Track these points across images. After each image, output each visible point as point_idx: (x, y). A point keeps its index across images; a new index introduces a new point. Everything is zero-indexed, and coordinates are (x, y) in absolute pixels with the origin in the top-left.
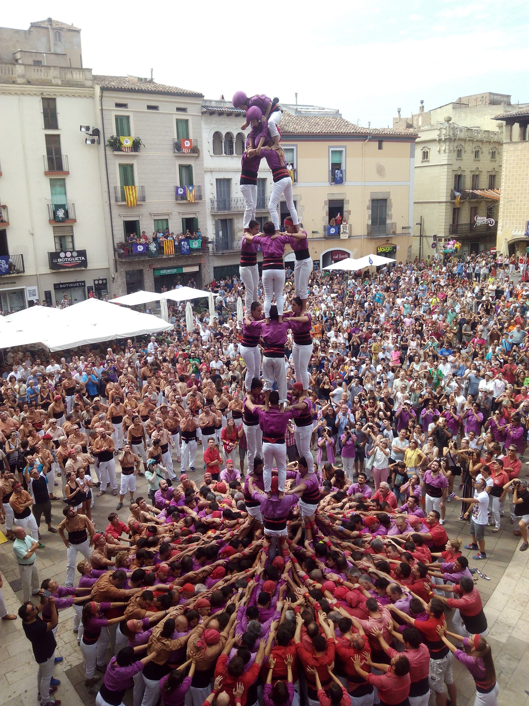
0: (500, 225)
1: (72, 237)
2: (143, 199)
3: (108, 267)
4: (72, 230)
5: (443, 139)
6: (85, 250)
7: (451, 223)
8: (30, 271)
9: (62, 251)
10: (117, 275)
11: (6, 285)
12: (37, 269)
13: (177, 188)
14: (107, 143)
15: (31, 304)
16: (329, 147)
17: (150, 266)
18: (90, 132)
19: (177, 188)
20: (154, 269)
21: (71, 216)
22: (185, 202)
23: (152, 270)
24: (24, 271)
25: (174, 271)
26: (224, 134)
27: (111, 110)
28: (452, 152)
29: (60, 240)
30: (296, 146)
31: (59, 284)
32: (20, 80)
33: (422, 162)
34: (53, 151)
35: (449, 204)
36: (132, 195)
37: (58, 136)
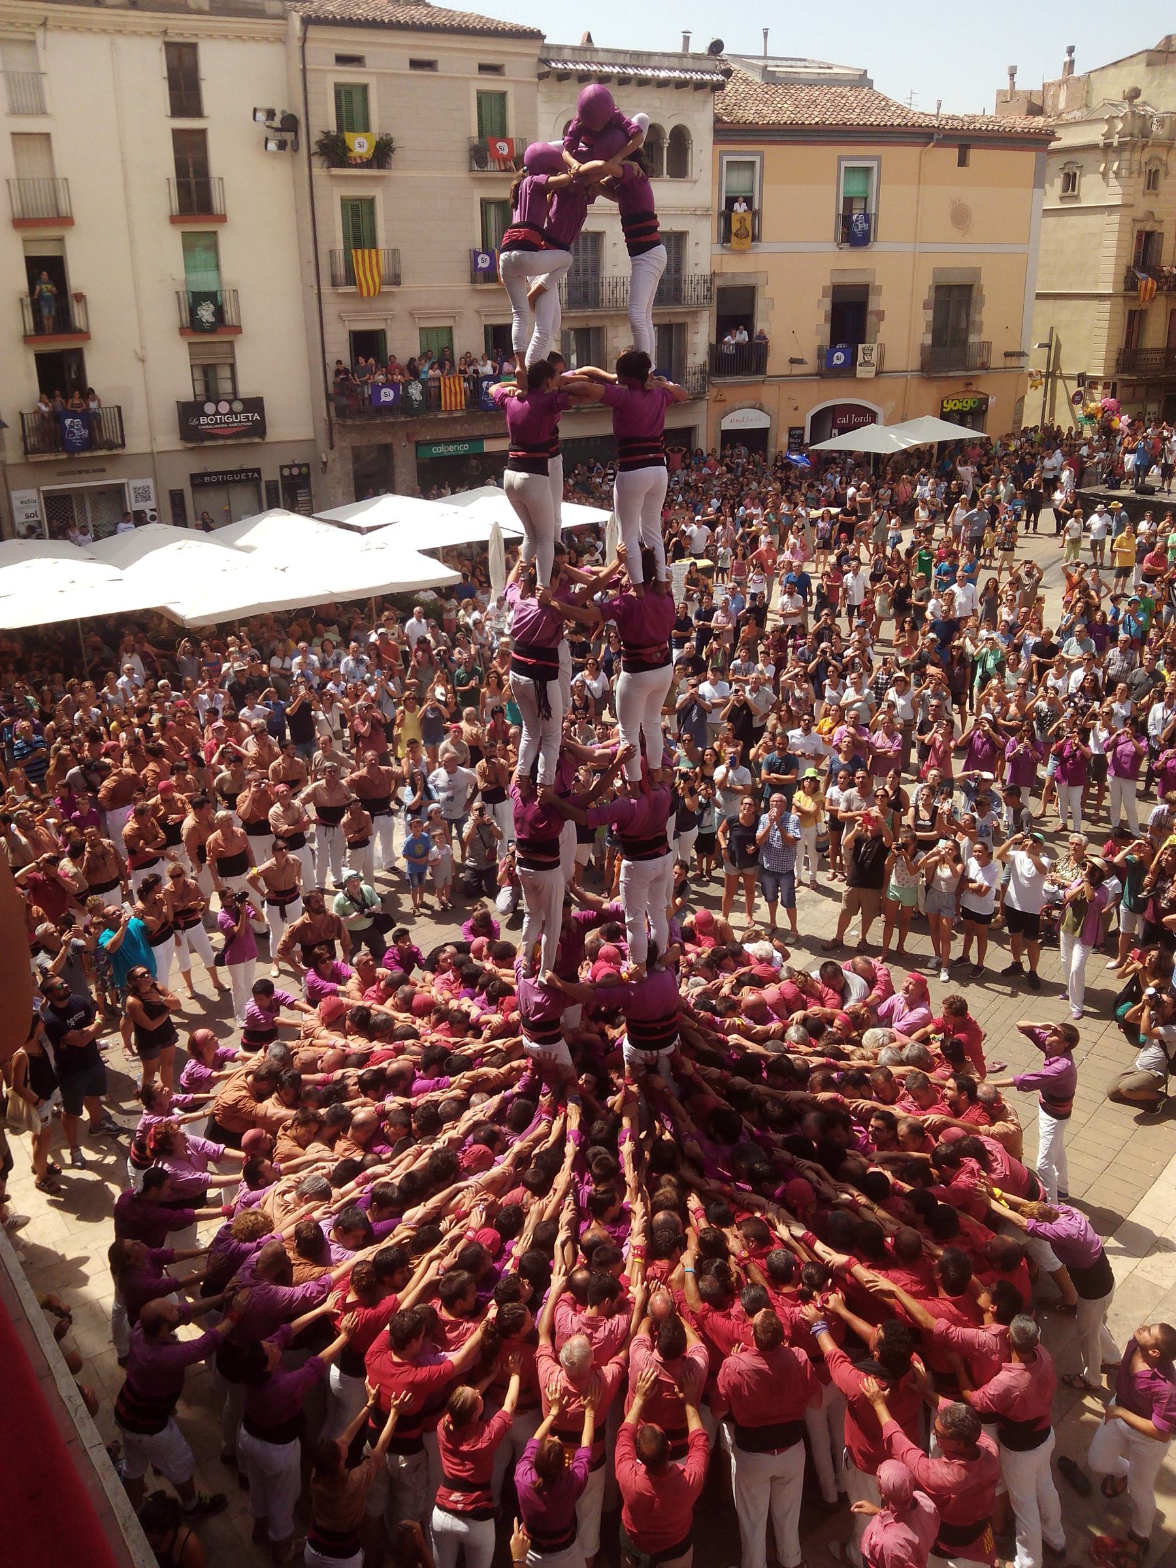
1: (232, 367)
2: (396, 280)
3: (312, 437)
4: (232, 353)
6: (262, 398)
8: (136, 443)
9: (209, 400)
10: (332, 455)
11: (84, 476)
12: (152, 439)
13: (476, 254)
14: (314, 148)
15: (140, 519)
16: (841, 158)
17: (408, 436)
18: (277, 123)
19: (476, 254)
20: (418, 443)
21: (230, 317)
22: (493, 286)
23: (413, 446)
24: (123, 445)
25: (463, 448)
27: (324, 71)
29: (206, 374)
30: (761, 154)
31: (201, 476)
34: (191, 169)
36: (370, 267)
37: (203, 132)
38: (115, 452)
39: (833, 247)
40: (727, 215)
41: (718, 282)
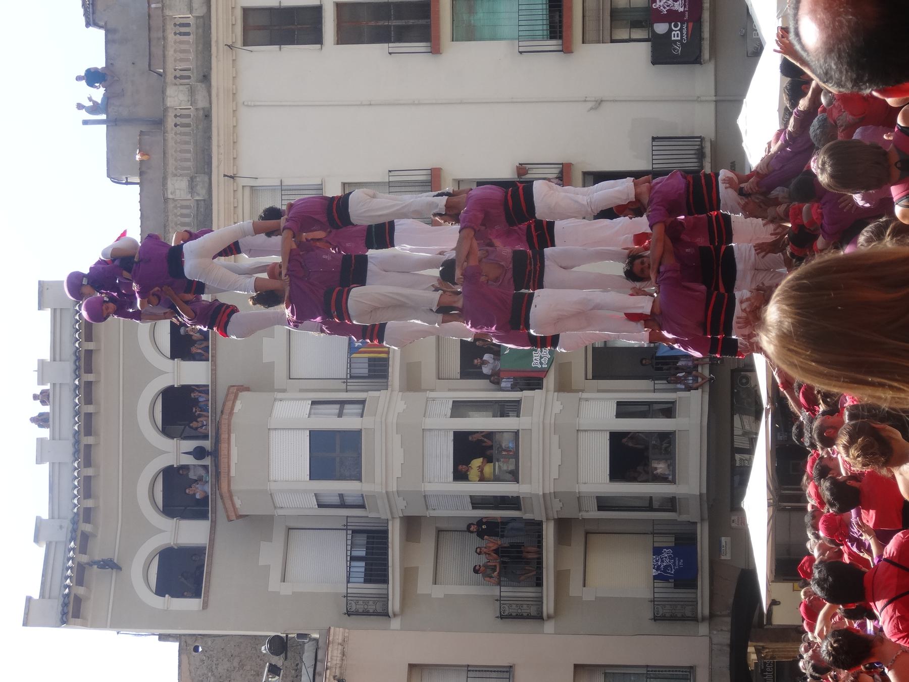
12: (698, 100)
32: (202, 103)
34: (381, 23)
38: (708, 150)
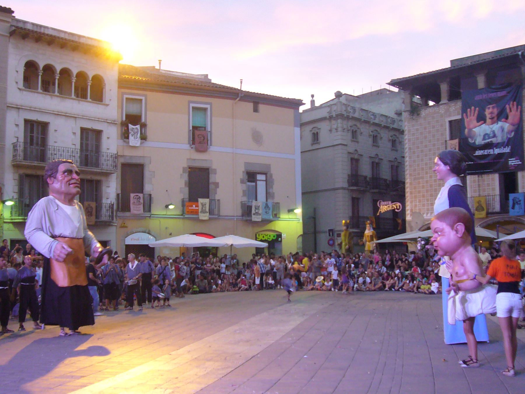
0: (408, 207)
5: (334, 116)
7: (351, 214)
16: (190, 102)
26: (41, 65)
28: (345, 130)
33: (312, 144)
35: (346, 191)
39: (187, 146)
40: (125, 125)
41: (122, 160)
